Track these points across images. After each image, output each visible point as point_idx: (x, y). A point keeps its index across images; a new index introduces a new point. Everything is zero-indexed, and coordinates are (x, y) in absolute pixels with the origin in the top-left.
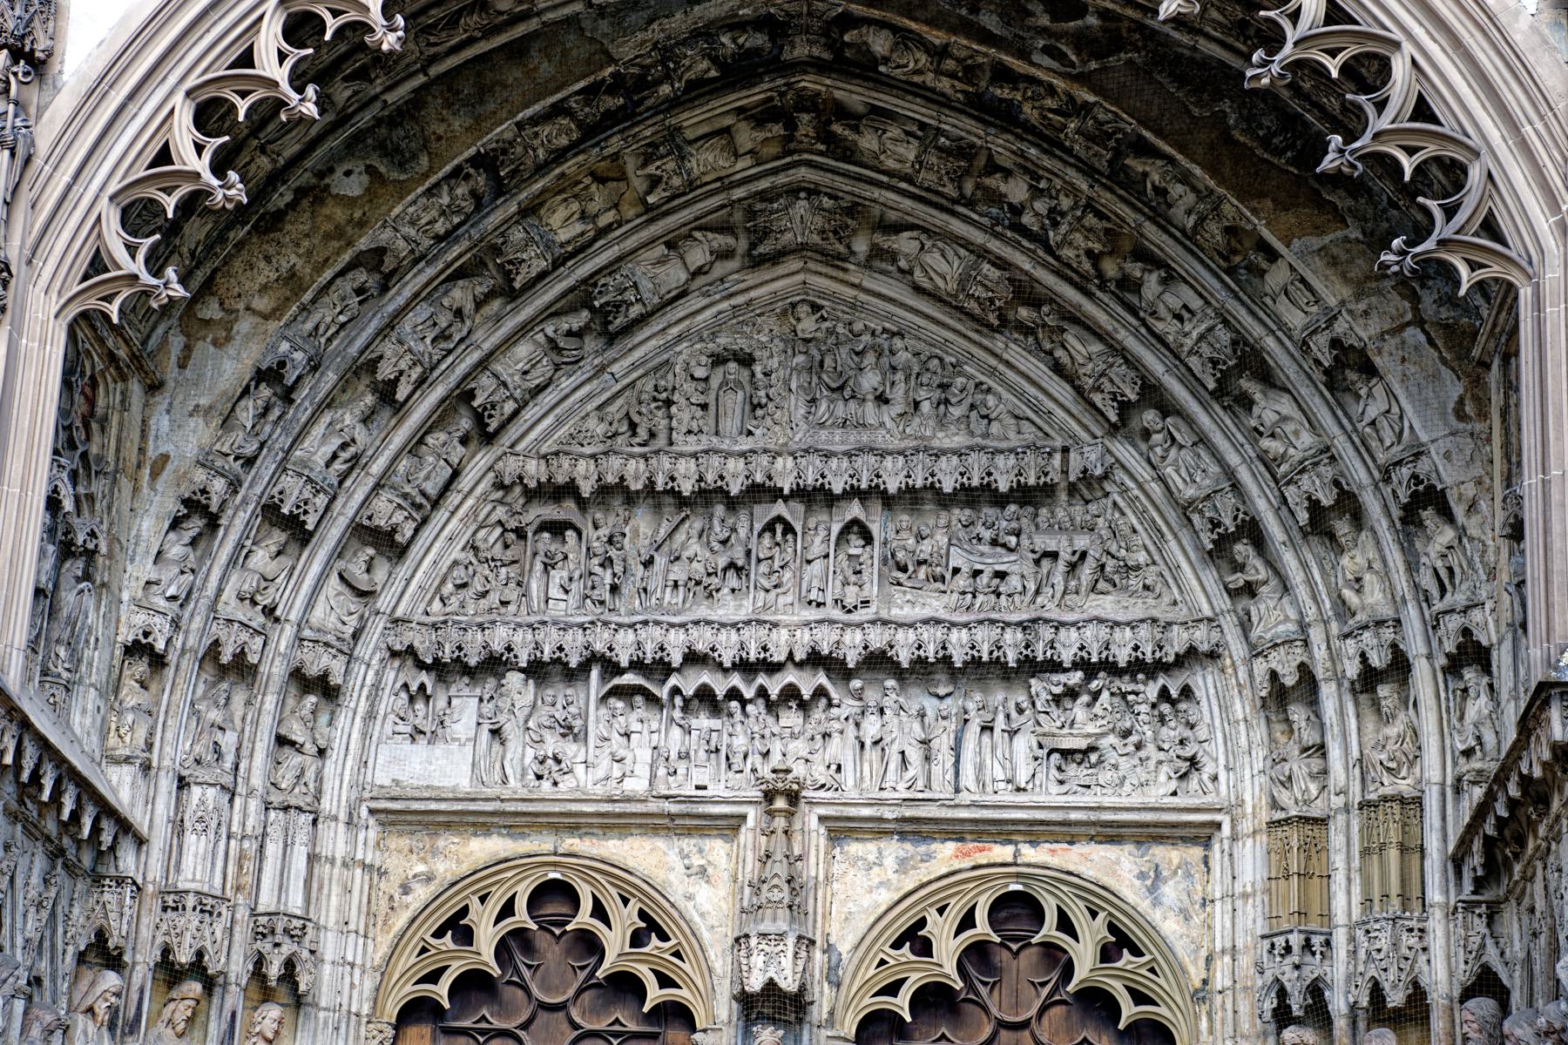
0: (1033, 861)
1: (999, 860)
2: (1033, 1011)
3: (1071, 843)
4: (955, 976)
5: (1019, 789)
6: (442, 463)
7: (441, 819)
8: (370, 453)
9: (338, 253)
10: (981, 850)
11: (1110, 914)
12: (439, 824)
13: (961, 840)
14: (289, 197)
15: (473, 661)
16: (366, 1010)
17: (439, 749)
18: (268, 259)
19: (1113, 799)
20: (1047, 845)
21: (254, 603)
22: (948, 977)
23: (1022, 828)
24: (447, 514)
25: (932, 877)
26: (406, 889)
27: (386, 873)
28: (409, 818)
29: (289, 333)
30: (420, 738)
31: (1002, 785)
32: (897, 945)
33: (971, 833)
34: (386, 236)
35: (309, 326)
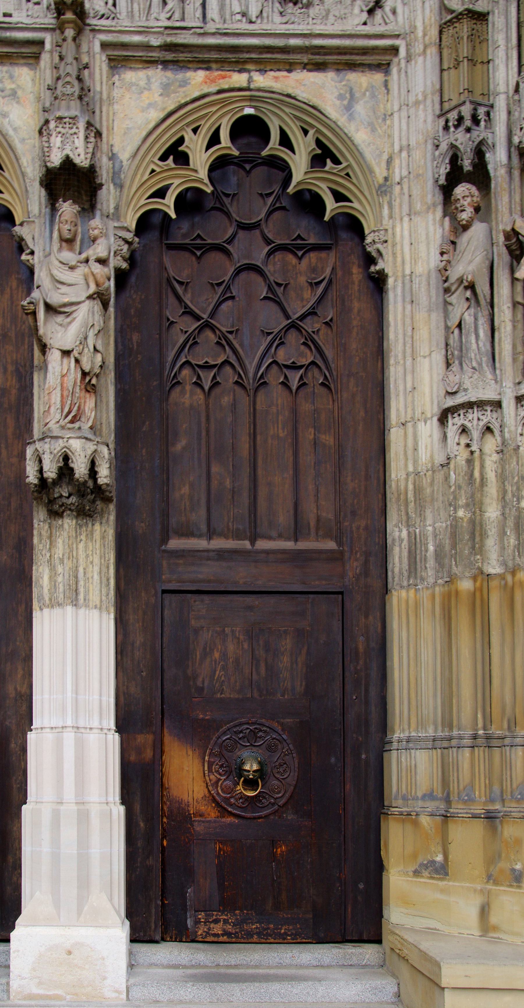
0: (262, 85)
1: (237, 86)
2: (263, 215)
3: (289, 71)
4: (206, 181)
5: (251, 22)
10: (224, 77)
11: (318, 131)
13: (208, 69)
19: (322, 27)
20: (272, 73)
22: (201, 181)
23: (253, 56)
25: (188, 99)
31: (239, 17)
32: (163, 158)
33: (216, 61)
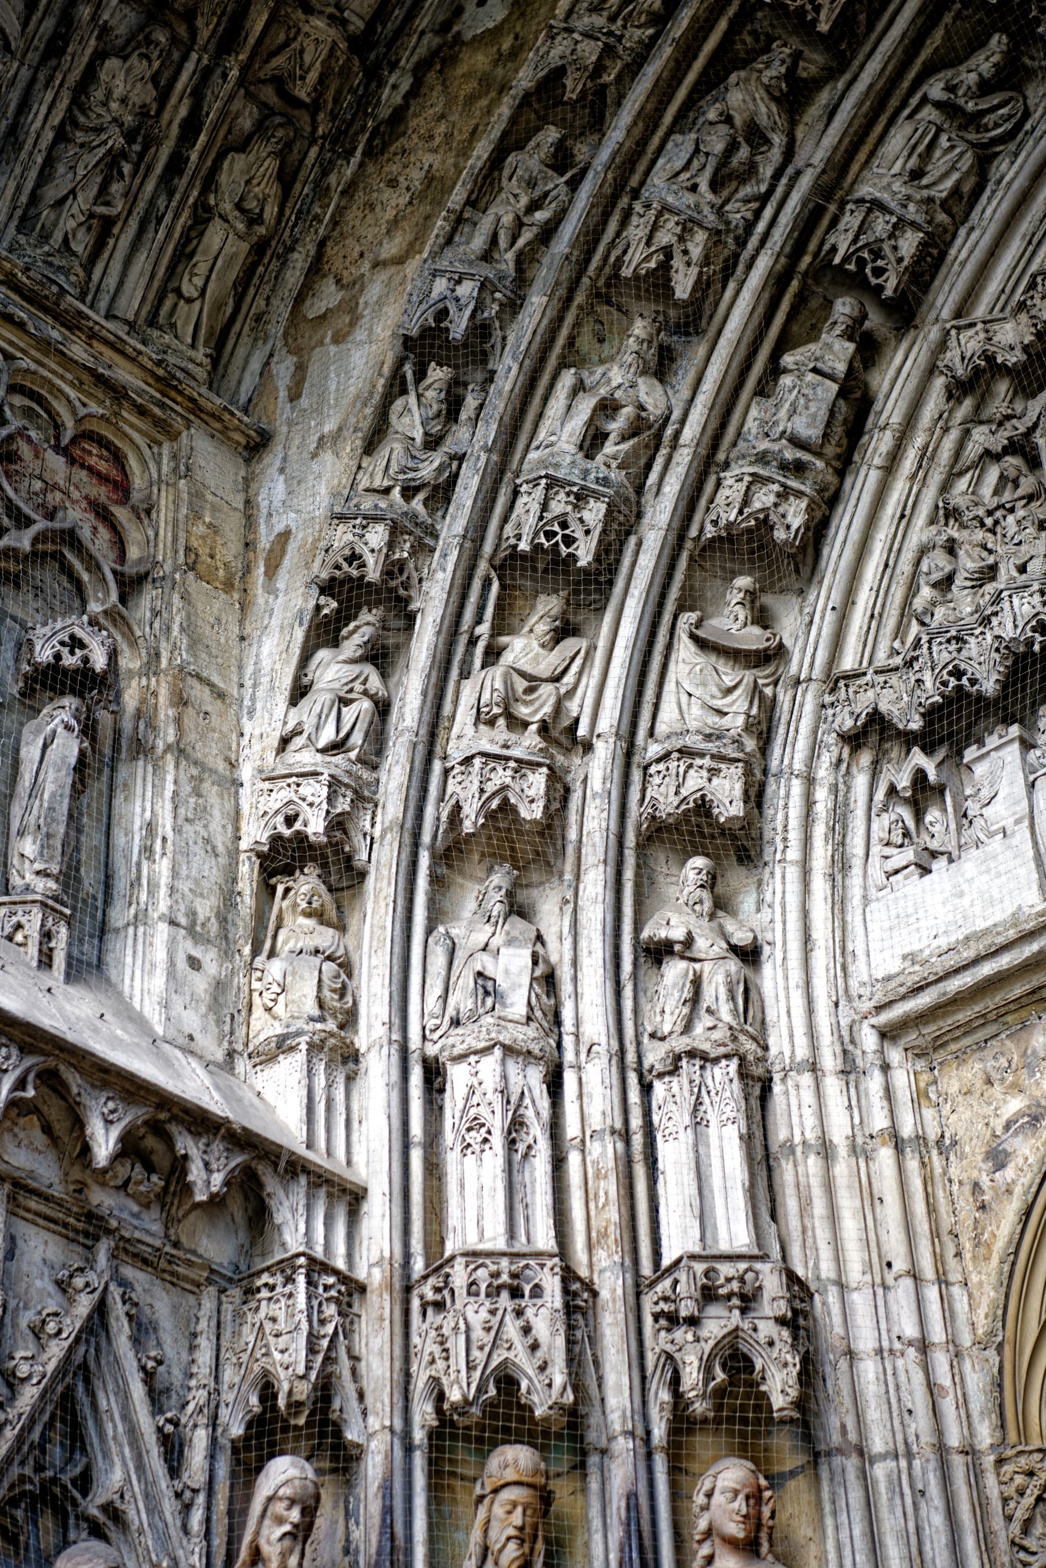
6: (810, 377)
7: (1018, 990)
8: (676, 415)
9: (489, 111)
12: (1020, 1004)
14: (405, 85)
15: (989, 686)
16: (985, 1435)
17: (970, 864)
18: (393, 183)
21: (516, 724)
24: (874, 476)
26: (998, 1159)
27: (955, 1143)
28: (962, 1016)
29: (443, 264)
30: (939, 865)
34: (558, 51)
35: (478, 242)
